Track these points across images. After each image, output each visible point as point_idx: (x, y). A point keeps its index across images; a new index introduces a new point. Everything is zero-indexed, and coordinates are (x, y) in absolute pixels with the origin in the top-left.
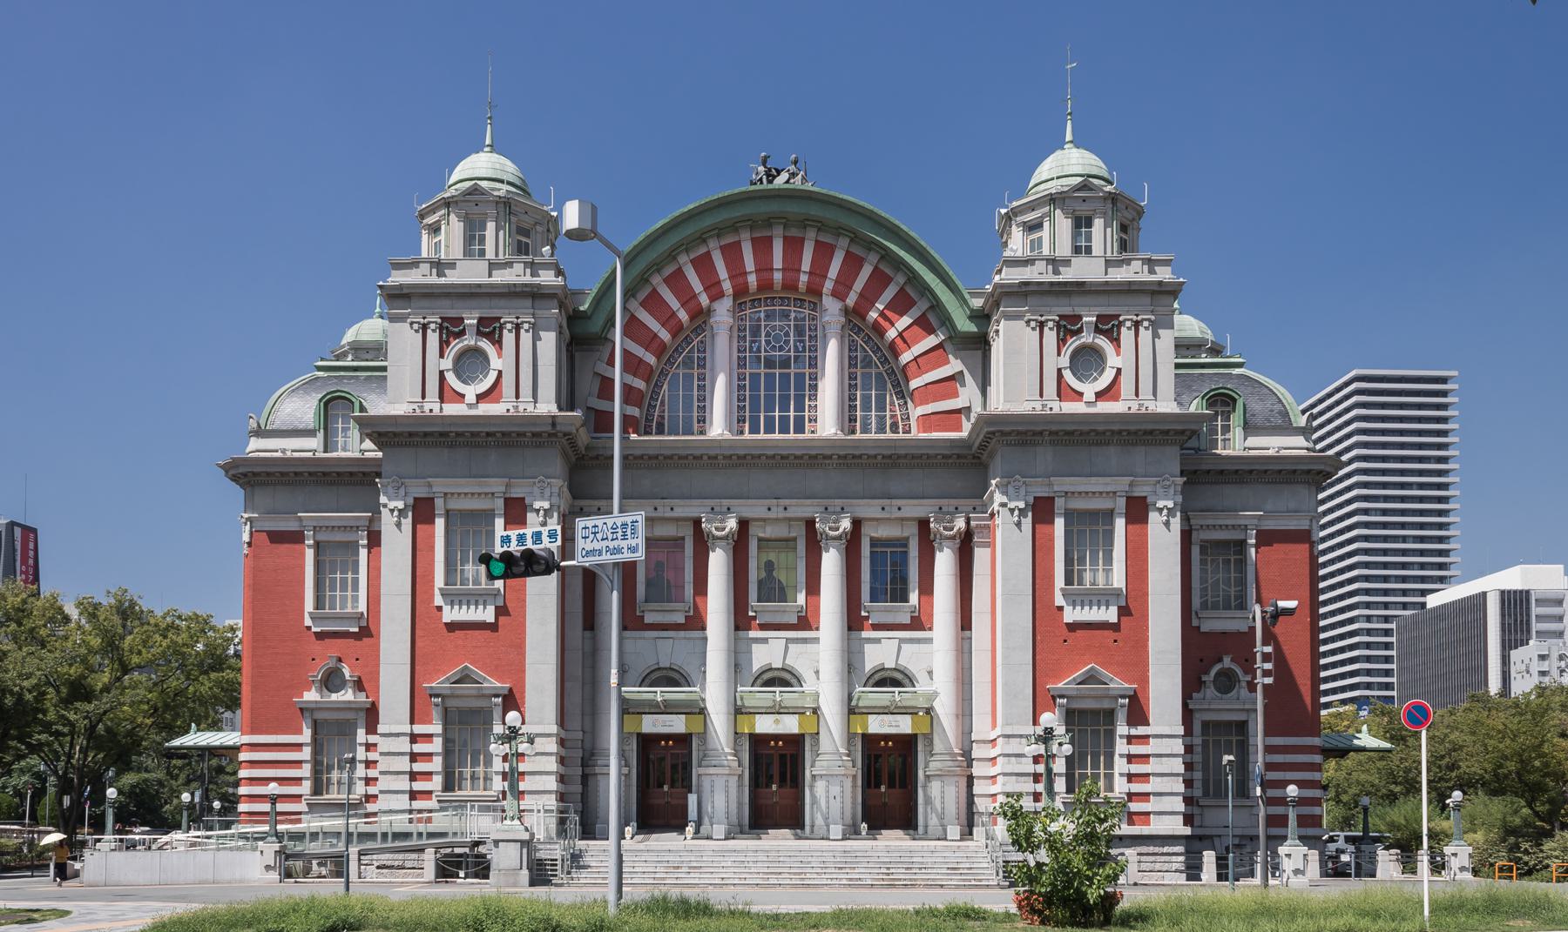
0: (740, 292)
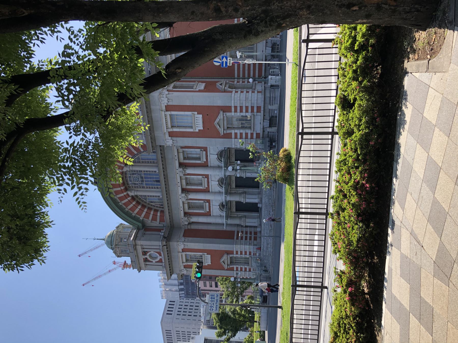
0: (126, 189)
